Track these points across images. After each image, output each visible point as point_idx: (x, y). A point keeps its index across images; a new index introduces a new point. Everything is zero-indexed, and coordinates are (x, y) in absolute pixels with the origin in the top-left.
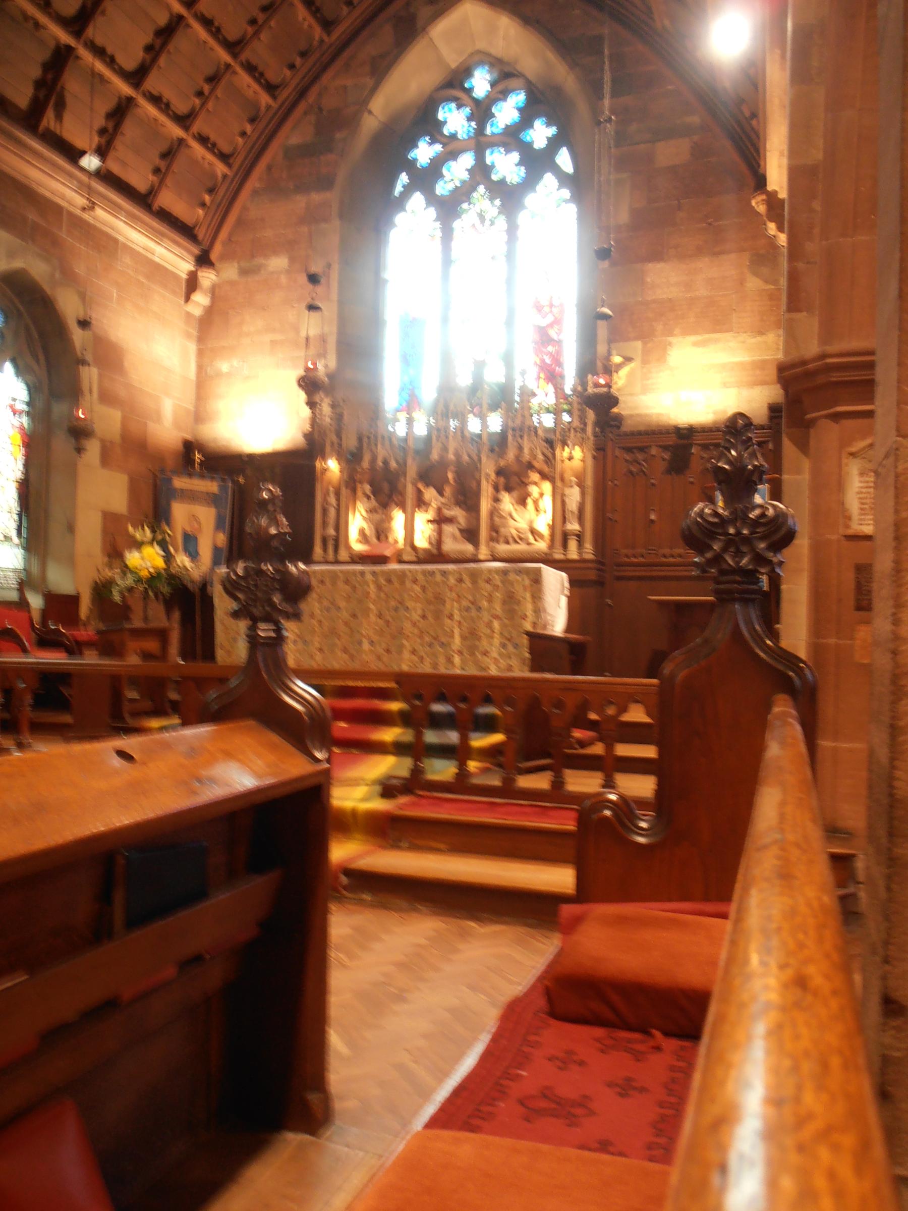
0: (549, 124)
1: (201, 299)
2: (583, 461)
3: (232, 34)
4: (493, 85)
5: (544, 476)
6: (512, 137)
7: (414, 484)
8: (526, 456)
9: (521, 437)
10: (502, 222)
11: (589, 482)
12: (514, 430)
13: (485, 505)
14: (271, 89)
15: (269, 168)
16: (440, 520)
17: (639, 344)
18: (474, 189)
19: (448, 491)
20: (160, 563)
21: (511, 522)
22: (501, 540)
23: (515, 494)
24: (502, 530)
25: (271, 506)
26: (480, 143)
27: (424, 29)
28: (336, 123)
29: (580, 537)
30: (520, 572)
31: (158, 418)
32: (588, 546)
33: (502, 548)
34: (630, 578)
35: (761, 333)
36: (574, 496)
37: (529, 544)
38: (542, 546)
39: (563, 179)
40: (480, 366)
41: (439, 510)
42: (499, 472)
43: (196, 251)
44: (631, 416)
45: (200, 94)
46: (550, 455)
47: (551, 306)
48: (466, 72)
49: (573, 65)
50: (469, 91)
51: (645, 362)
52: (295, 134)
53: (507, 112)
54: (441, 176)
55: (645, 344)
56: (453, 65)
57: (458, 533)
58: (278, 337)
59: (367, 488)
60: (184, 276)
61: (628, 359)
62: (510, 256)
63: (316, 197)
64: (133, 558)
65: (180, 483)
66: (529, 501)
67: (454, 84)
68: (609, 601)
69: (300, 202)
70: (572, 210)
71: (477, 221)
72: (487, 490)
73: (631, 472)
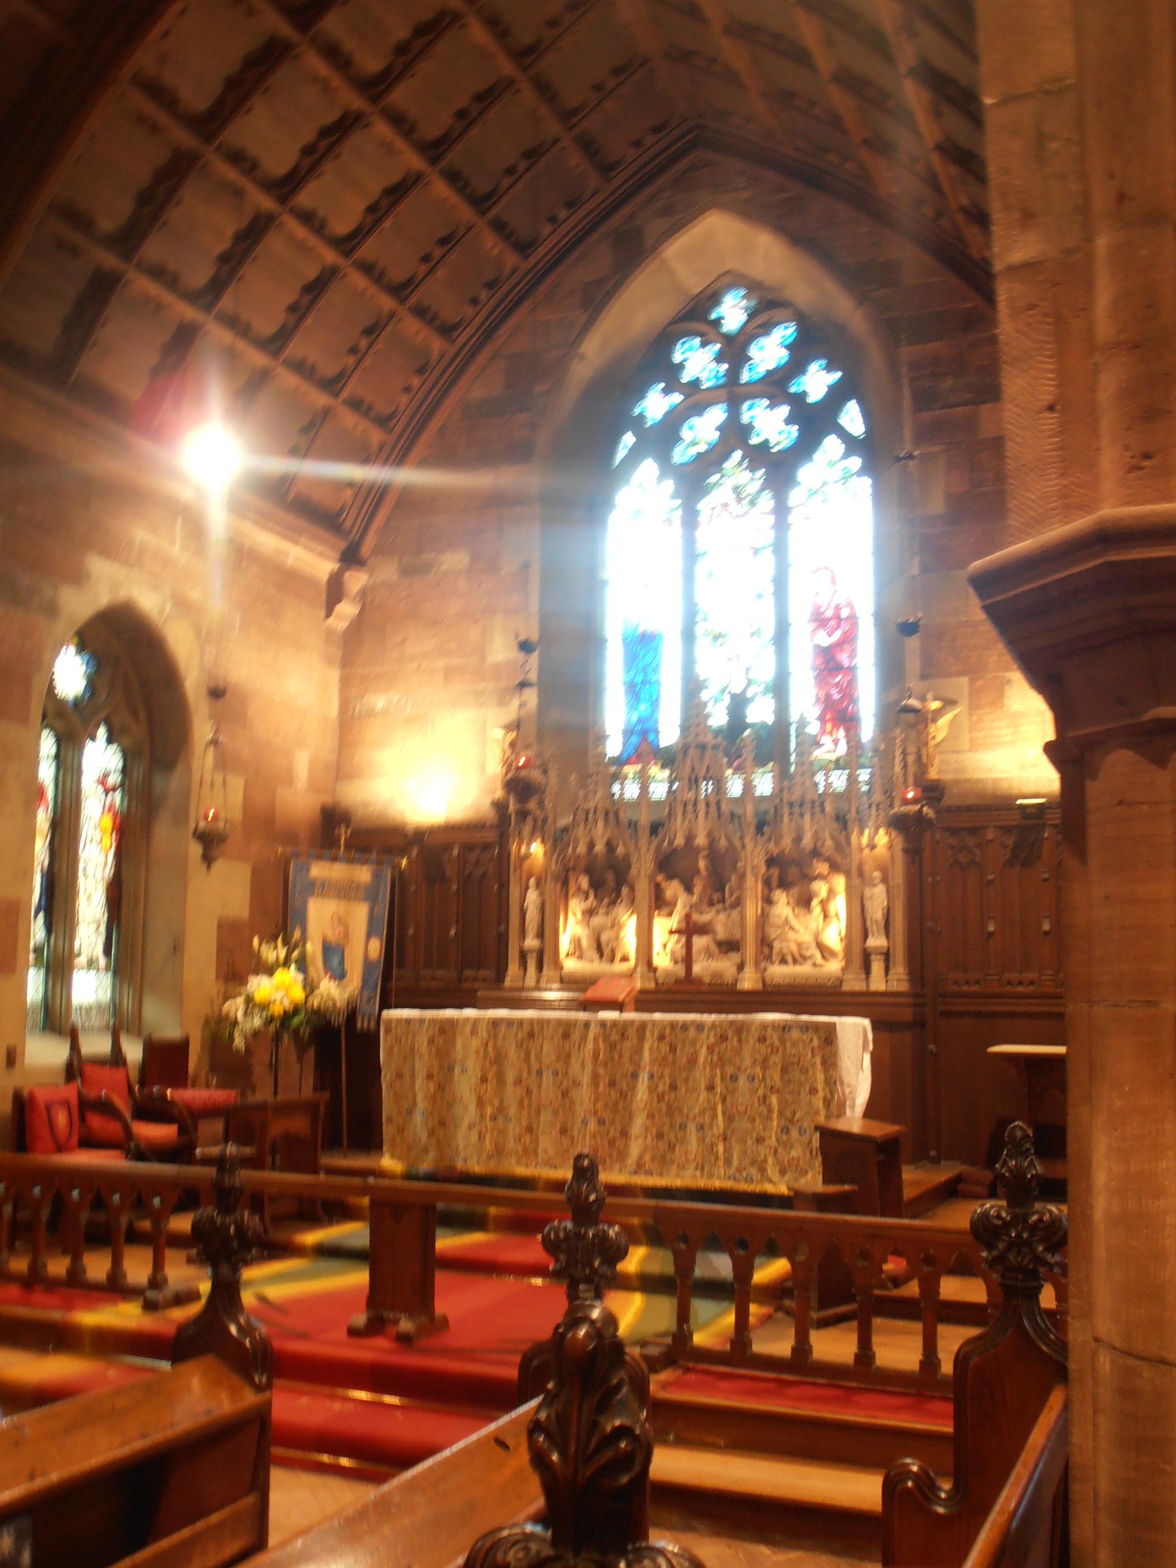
0: (829, 368)
1: (347, 610)
2: (890, 847)
3: (397, 274)
4: (751, 317)
5: (835, 868)
6: (776, 386)
7: (652, 878)
8: (807, 841)
9: (802, 815)
10: (767, 501)
11: (898, 876)
12: (791, 804)
13: (752, 909)
14: (447, 331)
15: (442, 431)
16: (689, 930)
17: (964, 681)
18: (726, 456)
19: (697, 890)
20: (298, 994)
21: (791, 935)
23: (795, 891)
24: (777, 945)
25: (450, 909)
26: (733, 392)
27: (655, 248)
28: (533, 374)
29: (887, 956)
30: (806, 1027)
31: (290, 780)
32: (900, 970)
33: (778, 972)
34: (961, 1015)
36: (877, 898)
37: (815, 965)
38: (834, 967)
39: (852, 445)
40: (738, 704)
41: (688, 917)
42: (771, 862)
43: (342, 545)
44: (957, 782)
45: (353, 350)
46: (843, 841)
47: (837, 617)
48: (713, 298)
49: (861, 300)
50: (717, 323)
51: (973, 707)
52: (478, 386)
53: (769, 352)
54: (679, 439)
55: (972, 681)
56: (697, 290)
57: (713, 947)
58: (455, 662)
59: (584, 882)
60: (324, 578)
61: (949, 703)
62: (780, 548)
64: (262, 987)
65: (319, 870)
66: (815, 902)
67: (695, 316)
68: (932, 1047)
70: (865, 484)
71: (732, 497)
72: (753, 888)
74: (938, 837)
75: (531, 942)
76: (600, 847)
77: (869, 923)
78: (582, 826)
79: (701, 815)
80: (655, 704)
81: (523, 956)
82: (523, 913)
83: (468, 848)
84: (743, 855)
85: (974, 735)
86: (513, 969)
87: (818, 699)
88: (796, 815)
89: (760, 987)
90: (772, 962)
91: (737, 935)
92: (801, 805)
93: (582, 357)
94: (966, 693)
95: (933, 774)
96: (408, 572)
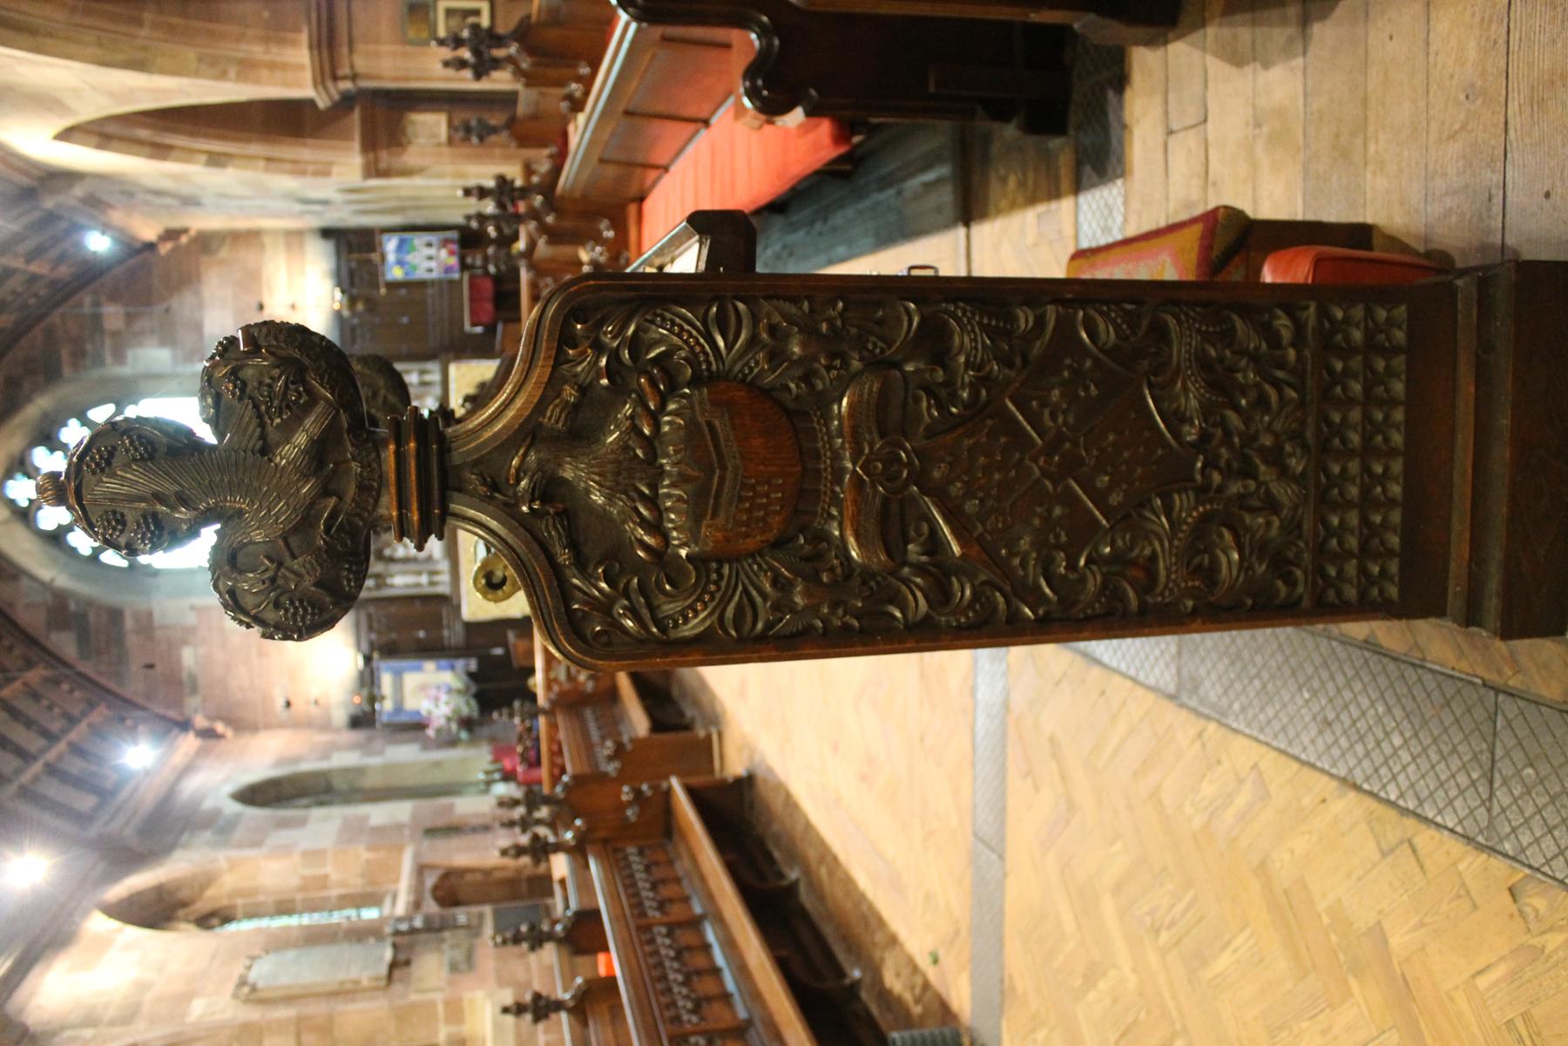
1: (220, 727)
28: (63, 611)
29: (422, 372)
35: (262, 246)
49: (29, 399)
63: (129, 623)
69: (132, 640)
75: (424, 579)
82: (407, 586)
83: (370, 628)
93: (52, 580)
96: (194, 690)
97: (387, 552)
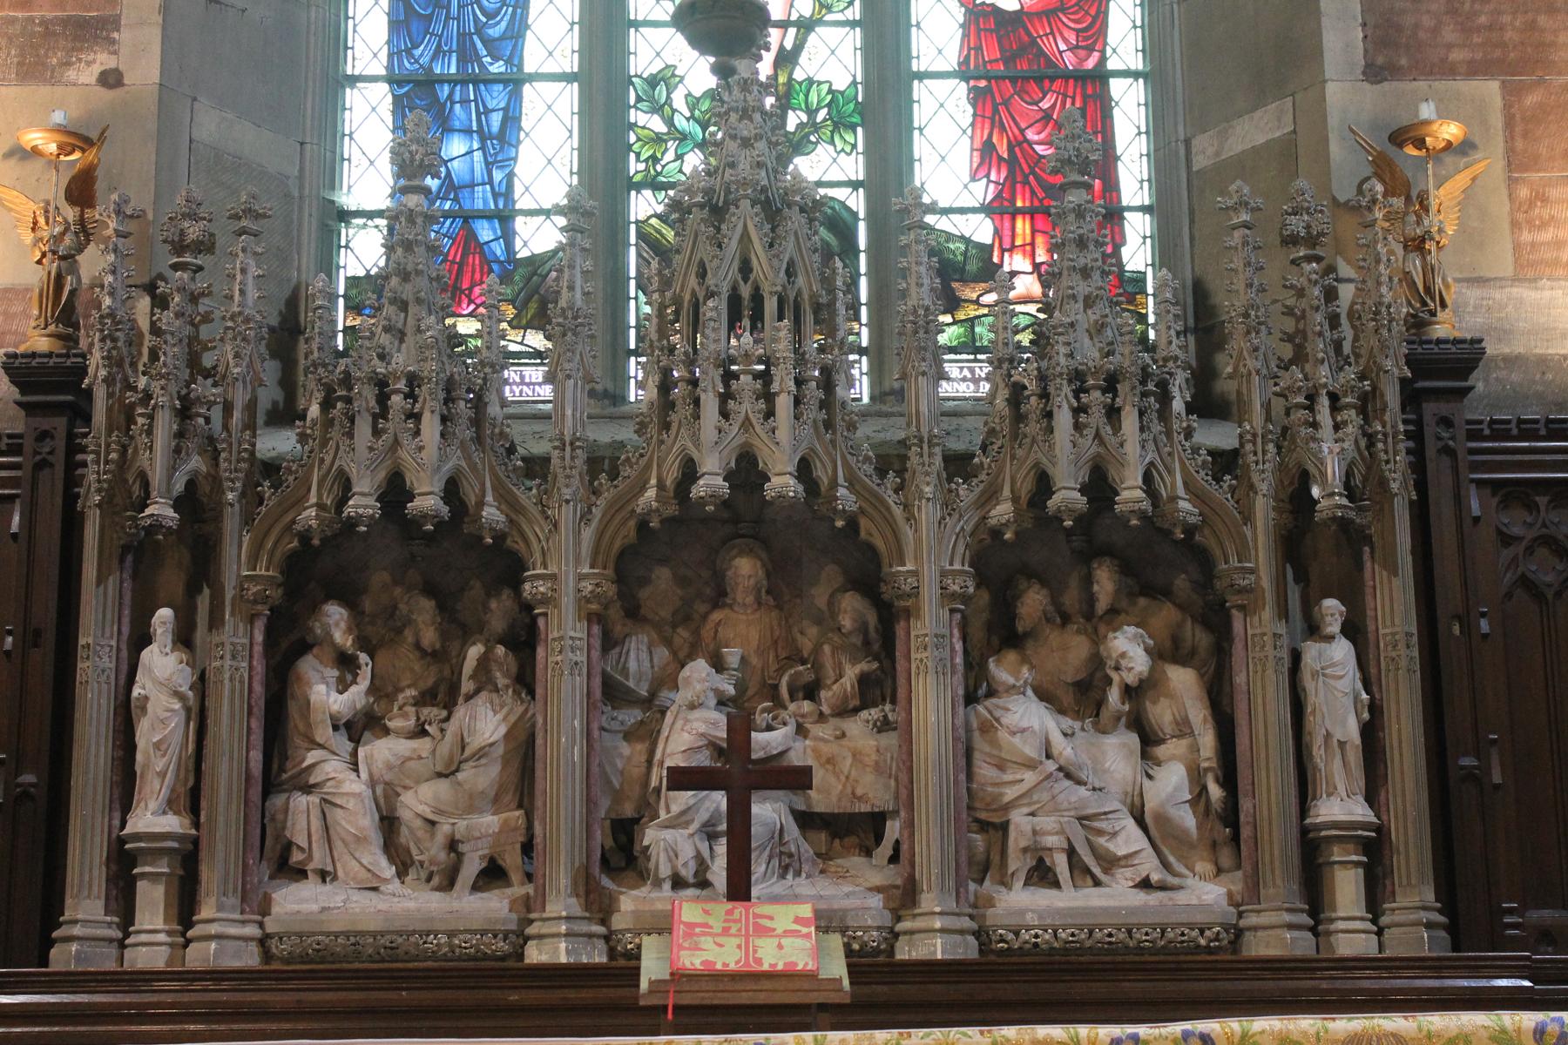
9: (1113, 413)
12: (1078, 378)
17: (1491, 89)
22: (1018, 864)
24: (1019, 820)
29: (1375, 850)
32: (1415, 900)
33: (1023, 907)
37: (1145, 884)
51: (1516, 163)
72: (931, 637)
73: (1525, 582)
74: (1475, 508)
75: (153, 818)
76: (427, 501)
77: (1318, 752)
78: (363, 428)
79: (784, 403)
80: (500, 141)
81: (123, 865)
82: (125, 716)
84: (908, 533)
85: (1526, 237)
86: (86, 909)
87: (986, 152)
88: (1096, 418)
89: (968, 950)
90: (1005, 882)
91: (874, 793)
92: (1111, 383)
94: (1497, 121)
95: (1443, 328)
97: (335, 621)
